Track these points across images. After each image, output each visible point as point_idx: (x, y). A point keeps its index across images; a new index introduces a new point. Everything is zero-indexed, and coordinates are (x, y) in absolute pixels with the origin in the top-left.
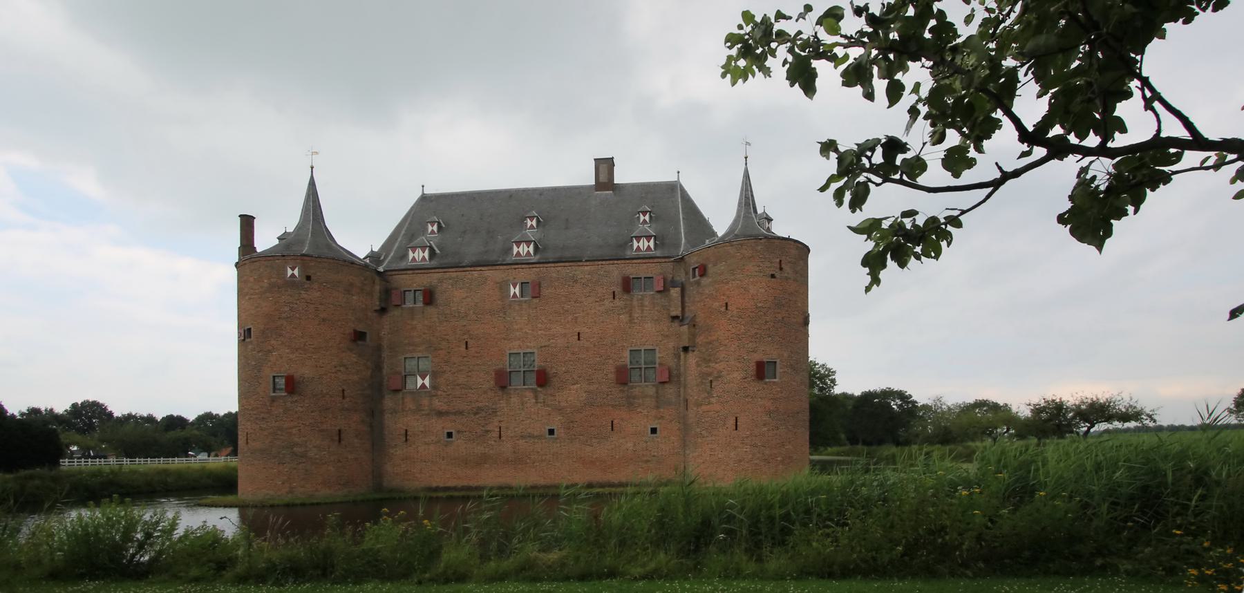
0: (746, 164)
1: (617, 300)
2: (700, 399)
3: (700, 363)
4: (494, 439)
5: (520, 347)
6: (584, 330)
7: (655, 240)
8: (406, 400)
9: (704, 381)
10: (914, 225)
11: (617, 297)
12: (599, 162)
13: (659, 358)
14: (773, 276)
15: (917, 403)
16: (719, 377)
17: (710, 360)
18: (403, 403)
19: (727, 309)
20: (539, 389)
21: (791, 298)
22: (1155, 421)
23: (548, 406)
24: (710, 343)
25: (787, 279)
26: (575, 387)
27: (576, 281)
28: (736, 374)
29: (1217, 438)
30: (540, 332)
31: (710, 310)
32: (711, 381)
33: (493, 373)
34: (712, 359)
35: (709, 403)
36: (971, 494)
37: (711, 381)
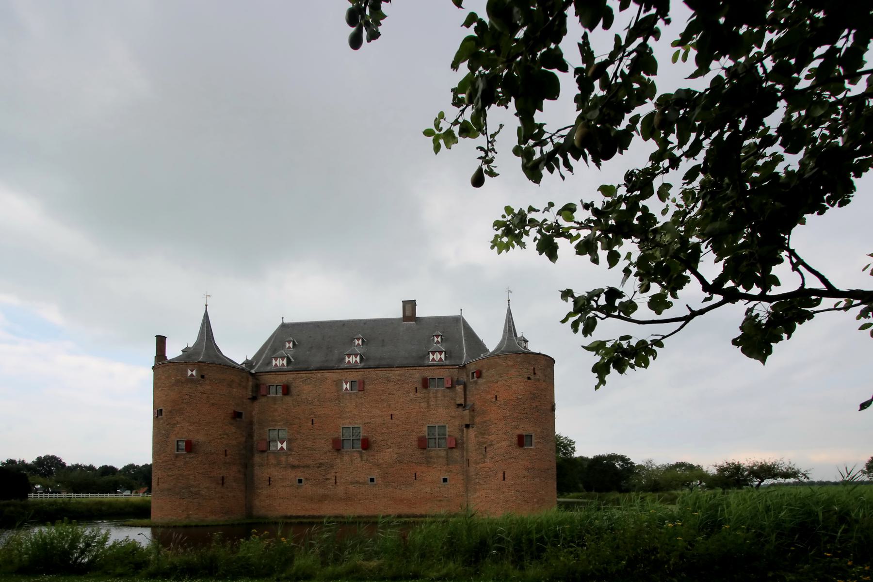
0: (509, 305)
1: (418, 393)
2: (478, 459)
3: (478, 435)
4: (331, 484)
5: (350, 423)
6: (395, 412)
7: (445, 354)
8: (269, 458)
9: (480, 447)
10: (629, 345)
11: (418, 391)
12: (405, 303)
13: (449, 431)
14: (529, 378)
15: (634, 464)
16: (492, 445)
17: (485, 434)
18: (268, 460)
19: (496, 400)
20: (363, 451)
21: (542, 393)
22: (808, 478)
23: (370, 463)
24: (485, 422)
25: (539, 380)
26: (389, 450)
27: (389, 381)
28: (503, 443)
29: (855, 490)
30: (364, 414)
31: (484, 400)
32: (486, 448)
33: (331, 441)
34: (486, 433)
35: (485, 462)
36: (675, 526)
37: (486, 448)
